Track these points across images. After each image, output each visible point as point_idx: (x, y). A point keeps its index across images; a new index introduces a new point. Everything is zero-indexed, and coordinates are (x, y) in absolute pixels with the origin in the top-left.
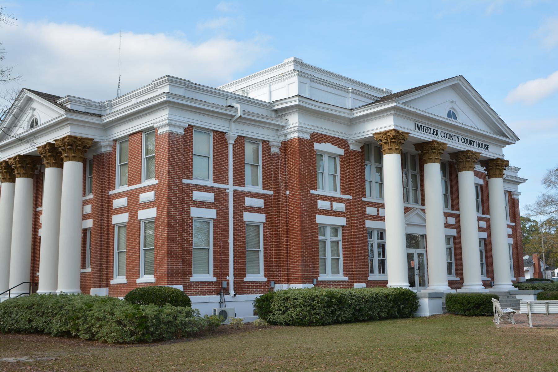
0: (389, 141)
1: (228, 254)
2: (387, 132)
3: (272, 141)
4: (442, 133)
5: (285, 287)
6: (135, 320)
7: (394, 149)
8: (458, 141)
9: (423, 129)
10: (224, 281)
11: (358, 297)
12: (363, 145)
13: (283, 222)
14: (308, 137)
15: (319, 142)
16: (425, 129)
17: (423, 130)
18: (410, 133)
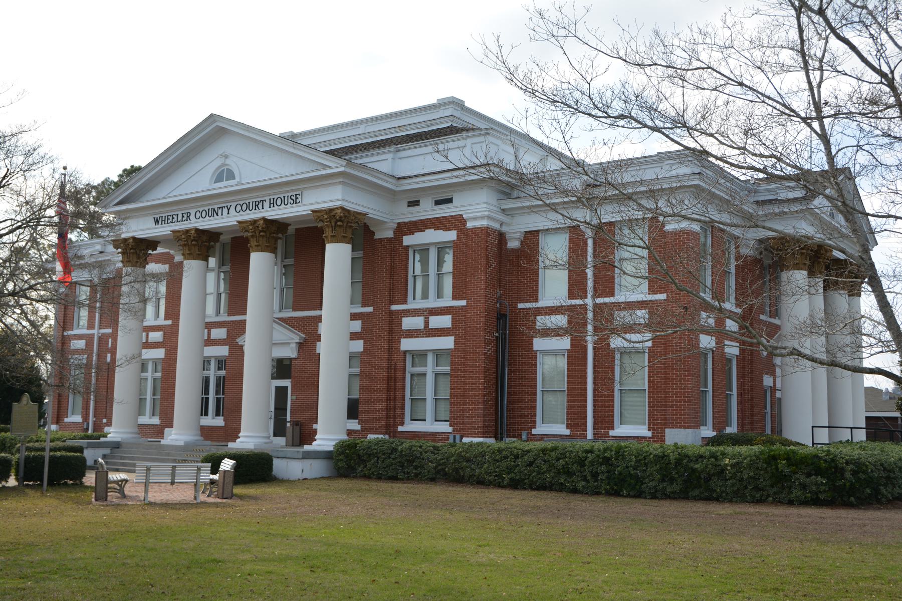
8: (228, 213)
9: (165, 221)
16: (166, 220)
17: (163, 222)
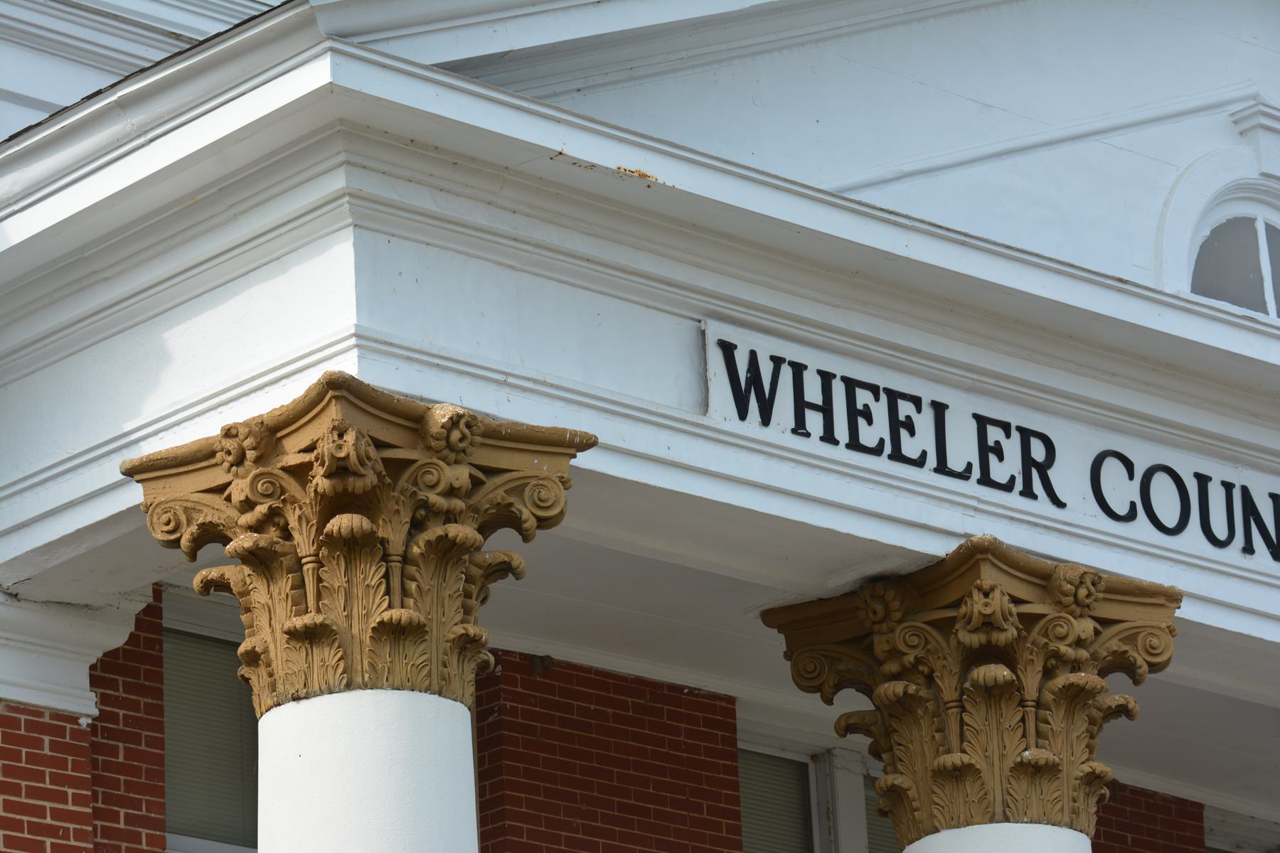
0: (303, 543)
4: (1112, 468)
7: (361, 630)
9: (826, 410)
12: (116, 637)
17: (814, 421)
18: (588, 443)
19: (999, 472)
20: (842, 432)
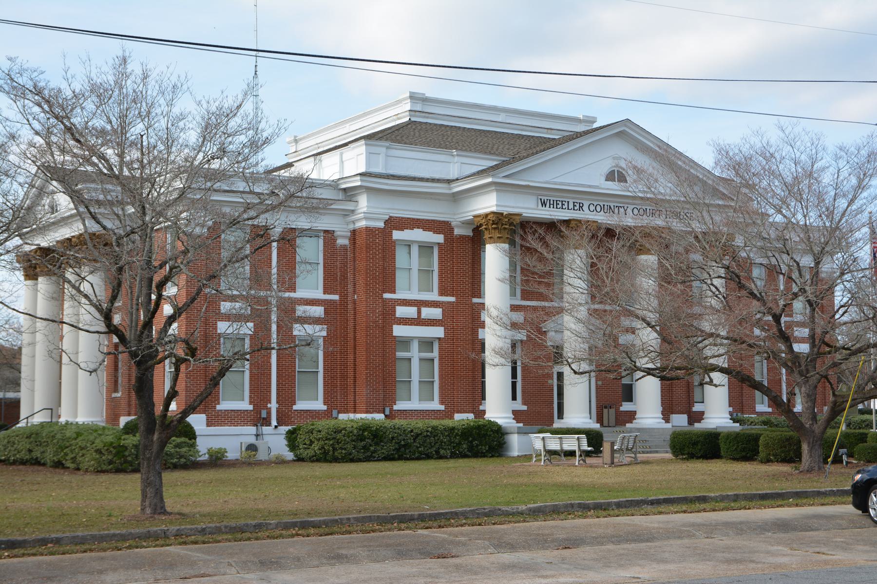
1: (270, 377)
2: (487, 215)
3: (337, 231)
5: (352, 416)
6: (112, 449)
7: (496, 237)
9: (553, 204)
10: (264, 409)
11: (404, 431)
13: (351, 335)
14: (381, 225)
15: (401, 229)
16: (554, 204)
17: (552, 206)
19: (576, 208)
20: (555, 207)
